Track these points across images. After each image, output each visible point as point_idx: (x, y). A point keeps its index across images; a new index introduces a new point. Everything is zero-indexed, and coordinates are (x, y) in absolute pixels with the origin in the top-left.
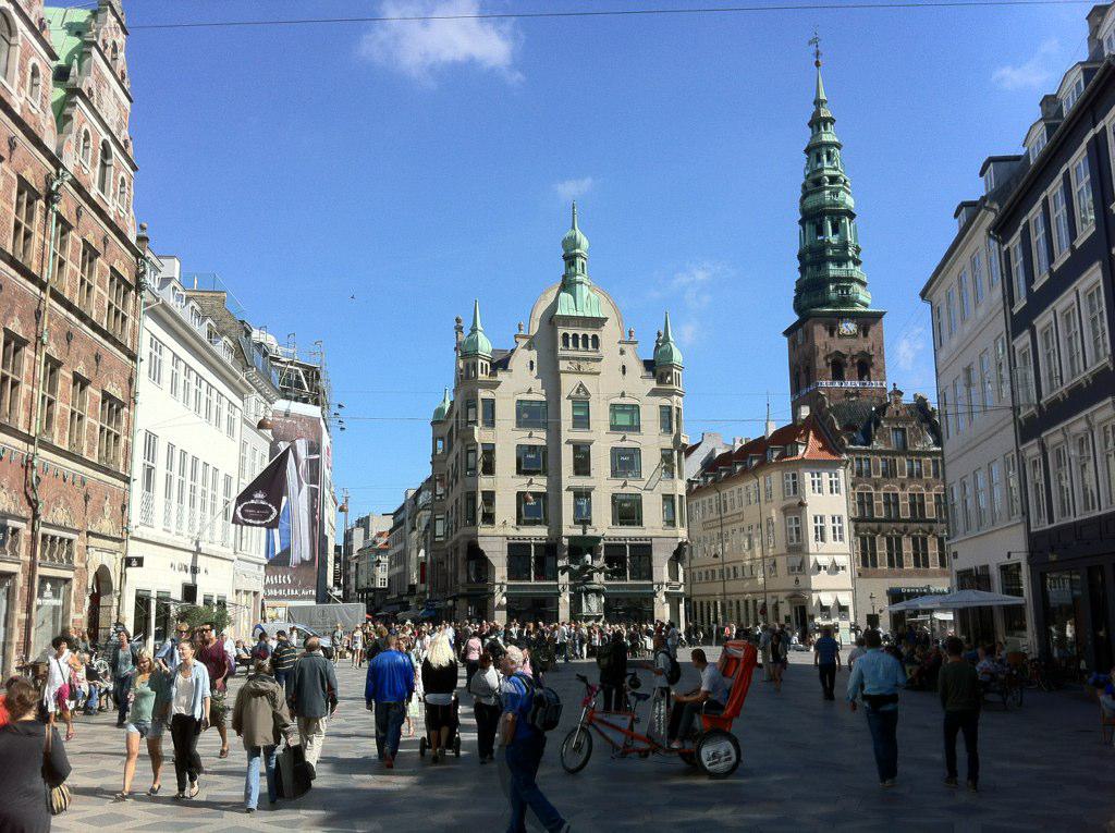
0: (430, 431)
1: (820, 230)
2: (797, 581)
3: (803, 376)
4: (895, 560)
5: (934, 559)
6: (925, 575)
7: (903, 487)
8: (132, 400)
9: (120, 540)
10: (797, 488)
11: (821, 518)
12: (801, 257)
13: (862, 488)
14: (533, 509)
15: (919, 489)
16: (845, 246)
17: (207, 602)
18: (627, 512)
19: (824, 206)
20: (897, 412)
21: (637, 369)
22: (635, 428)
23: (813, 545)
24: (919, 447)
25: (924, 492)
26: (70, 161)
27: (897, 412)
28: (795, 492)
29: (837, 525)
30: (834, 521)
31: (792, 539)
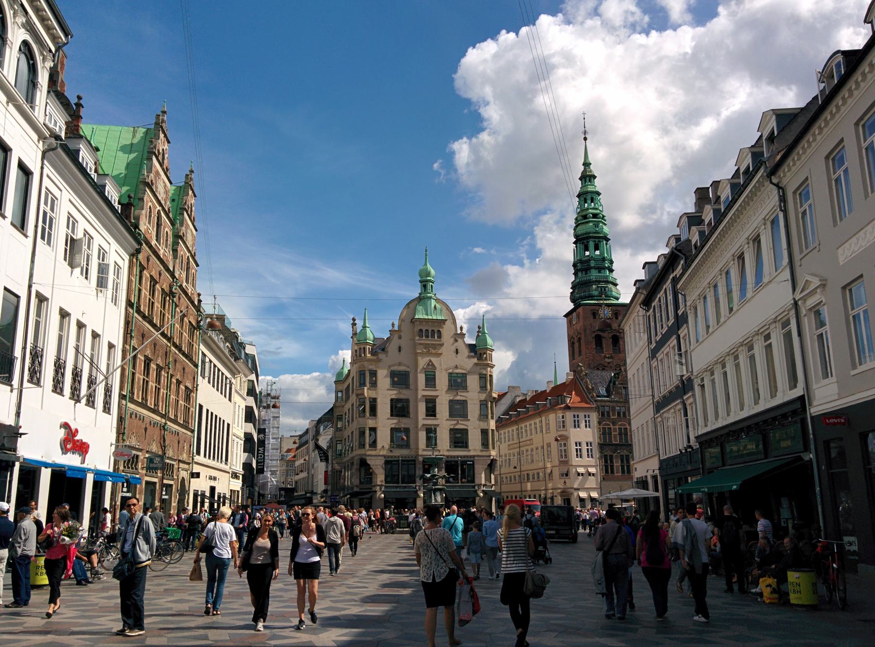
3: (576, 345)
8: (196, 388)
9: (188, 464)
12: (574, 265)
13: (605, 424)
16: (604, 259)
17: (219, 497)
18: (459, 439)
21: (465, 352)
23: (575, 460)
26: (177, 275)
28: (564, 426)
29: (589, 447)
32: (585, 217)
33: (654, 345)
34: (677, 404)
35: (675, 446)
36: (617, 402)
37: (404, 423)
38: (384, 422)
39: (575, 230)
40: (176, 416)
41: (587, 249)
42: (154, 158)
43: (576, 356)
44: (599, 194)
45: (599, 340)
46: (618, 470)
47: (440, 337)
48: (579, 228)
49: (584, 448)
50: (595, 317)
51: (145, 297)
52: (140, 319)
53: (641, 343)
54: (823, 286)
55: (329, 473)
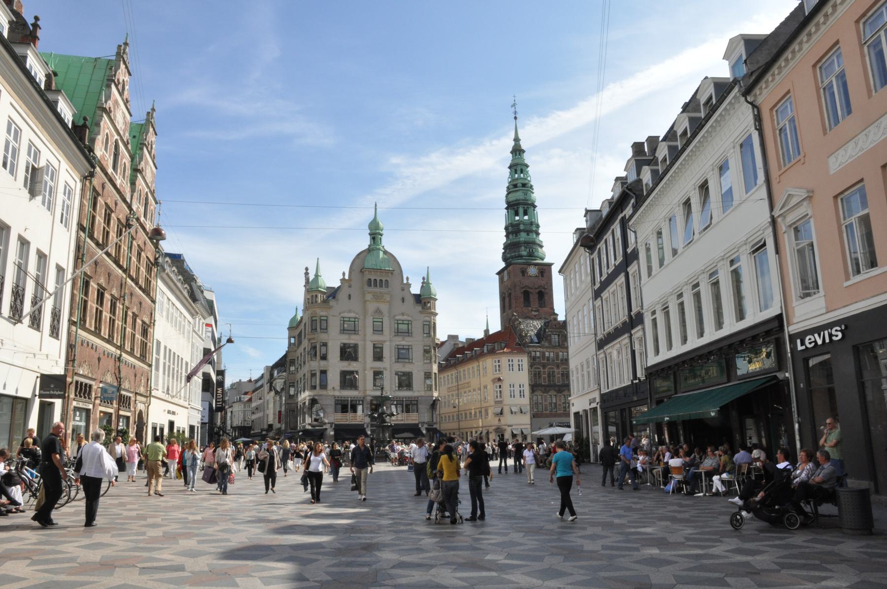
0: (286, 334)
3: (507, 300)
8: (153, 323)
9: (146, 397)
12: (506, 228)
14: (348, 380)
16: (531, 224)
17: (178, 431)
18: (405, 381)
21: (410, 301)
22: (408, 333)
23: (507, 400)
26: (134, 207)
32: (515, 186)
33: (598, 285)
34: (624, 339)
35: (620, 378)
37: (352, 366)
38: (335, 366)
40: (132, 349)
41: (517, 214)
42: (113, 86)
43: (507, 309)
44: (527, 166)
45: (526, 294)
47: (387, 286)
48: (510, 195)
49: (517, 389)
50: (523, 275)
51: (100, 224)
52: (93, 245)
53: (583, 286)
54: (809, 198)
55: (283, 412)
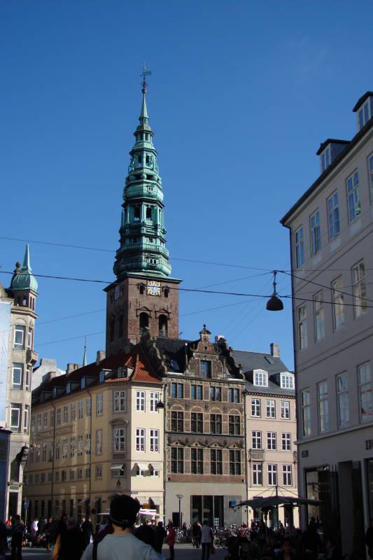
1: (138, 213)
2: (119, 483)
3: (117, 325)
4: (197, 468)
5: (226, 468)
6: (219, 481)
7: (206, 408)
10: (124, 406)
11: (142, 431)
12: (122, 231)
13: (175, 408)
15: (218, 411)
16: (155, 227)
19: (142, 196)
20: (206, 348)
24: (220, 376)
25: (222, 413)
27: (206, 348)
29: (154, 437)
30: (152, 435)
31: (117, 448)
36: (192, 379)
39: (125, 191)
45: (144, 319)
46: (187, 468)
48: (131, 189)
49: (148, 437)
50: (141, 293)
